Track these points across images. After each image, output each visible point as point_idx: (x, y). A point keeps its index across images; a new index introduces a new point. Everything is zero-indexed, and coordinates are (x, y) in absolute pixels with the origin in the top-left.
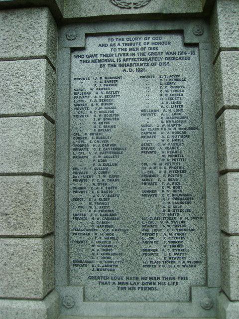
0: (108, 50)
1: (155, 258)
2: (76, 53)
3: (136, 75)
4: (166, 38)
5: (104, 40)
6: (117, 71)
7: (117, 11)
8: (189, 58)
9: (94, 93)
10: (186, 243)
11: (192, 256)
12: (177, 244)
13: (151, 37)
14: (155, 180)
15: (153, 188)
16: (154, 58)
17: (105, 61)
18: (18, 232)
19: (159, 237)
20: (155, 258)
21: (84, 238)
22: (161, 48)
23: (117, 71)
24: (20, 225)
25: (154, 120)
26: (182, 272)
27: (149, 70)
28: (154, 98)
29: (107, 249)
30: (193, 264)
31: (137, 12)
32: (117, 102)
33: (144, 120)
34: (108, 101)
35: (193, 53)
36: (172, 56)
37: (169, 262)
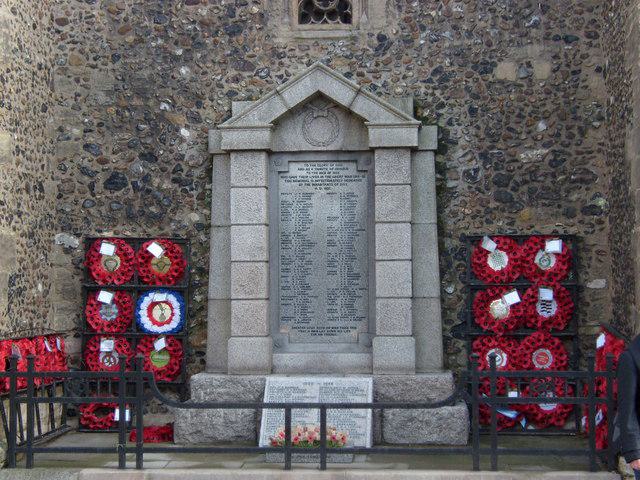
0: (304, 173)
1: (336, 315)
2: (282, 175)
3: (323, 192)
4: (345, 165)
5: (302, 165)
6: (311, 189)
7: (311, 148)
8: (361, 180)
9: (295, 204)
10: (356, 305)
11: (359, 314)
12: (350, 306)
13: (335, 164)
14: (336, 264)
15: (334, 269)
16: (337, 180)
17: (303, 181)
18: (251, 297)
19: (338, 302)
20: (336, 315)
21: (290, 302)
22: (342, 173)
23: (311, 189)
24: (252, 292)
25: (336, 224)
26: (352, 323)
27: (334, 189)
28: (335, 208)
29: (304, 309)
30: (360, 319)
31: (324, 149)
32: (312, 212)
33: (329, 224)
34: (304, 210)
35: (364, 177)
36: (349, 179)
37: (344, 317)
